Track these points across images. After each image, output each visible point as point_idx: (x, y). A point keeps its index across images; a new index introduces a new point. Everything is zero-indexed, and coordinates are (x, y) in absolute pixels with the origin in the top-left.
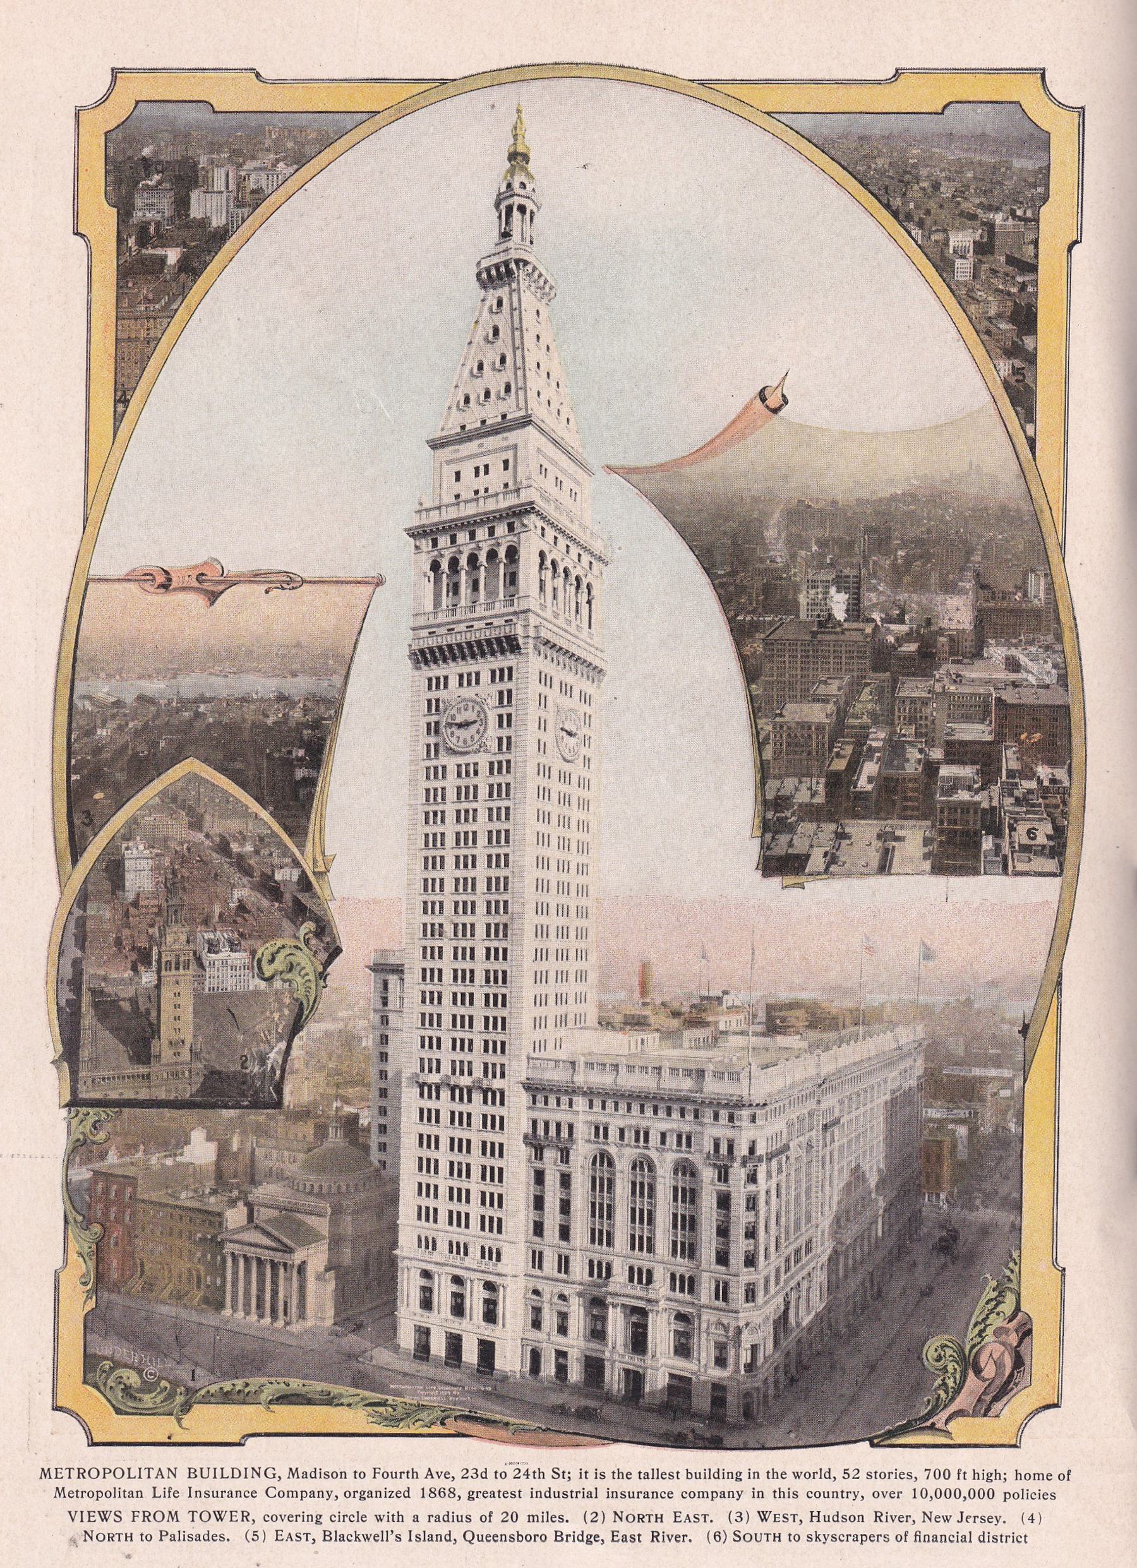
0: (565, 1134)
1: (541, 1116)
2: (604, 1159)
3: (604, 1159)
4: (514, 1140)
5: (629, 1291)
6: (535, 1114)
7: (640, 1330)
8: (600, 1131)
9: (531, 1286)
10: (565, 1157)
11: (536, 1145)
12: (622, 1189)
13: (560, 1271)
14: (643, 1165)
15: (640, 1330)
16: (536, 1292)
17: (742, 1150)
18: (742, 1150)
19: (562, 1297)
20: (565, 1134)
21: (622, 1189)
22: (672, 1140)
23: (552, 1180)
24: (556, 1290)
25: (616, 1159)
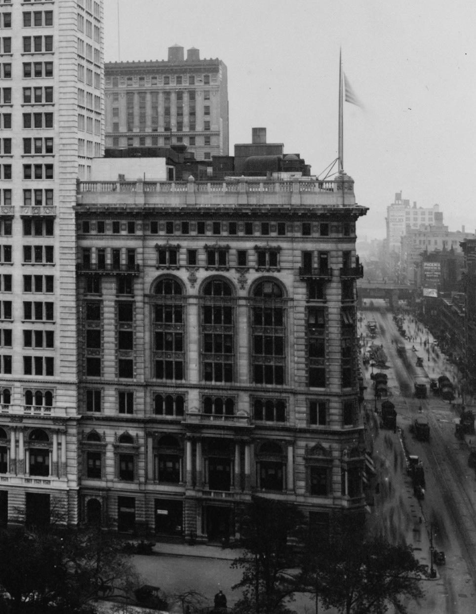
0: (124, 261)
1: (94, 243)
2: (168, 286)
3: (168, 286)
4: (63, 271)
5: (212, 421)
6: (86, 243)
7: (220, 468)
8: (168, 256)
9: (88, 430)
10: (125, 284)
11: (89, 277)
12: (192, 317)
13: (122, 410)
14: (216, 288)
15: (220, 468)
16: (95, 436)
17: (336, 265)
18: (336, 265)
19: (126, 438)
20: (124, 261)
21: (192, 317)
22: (252, 258)
23: (109, 313)
24: (120, 432)
25: (188, 284)
